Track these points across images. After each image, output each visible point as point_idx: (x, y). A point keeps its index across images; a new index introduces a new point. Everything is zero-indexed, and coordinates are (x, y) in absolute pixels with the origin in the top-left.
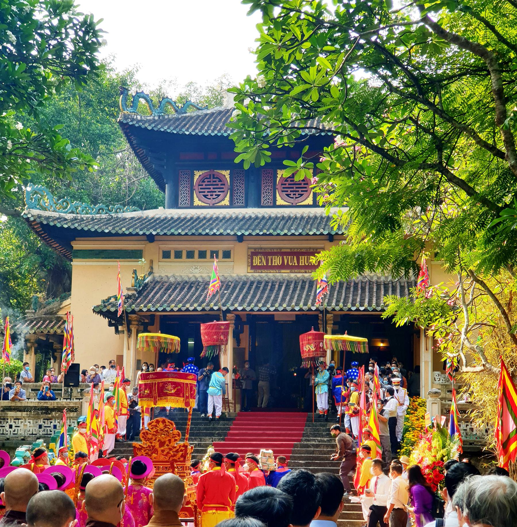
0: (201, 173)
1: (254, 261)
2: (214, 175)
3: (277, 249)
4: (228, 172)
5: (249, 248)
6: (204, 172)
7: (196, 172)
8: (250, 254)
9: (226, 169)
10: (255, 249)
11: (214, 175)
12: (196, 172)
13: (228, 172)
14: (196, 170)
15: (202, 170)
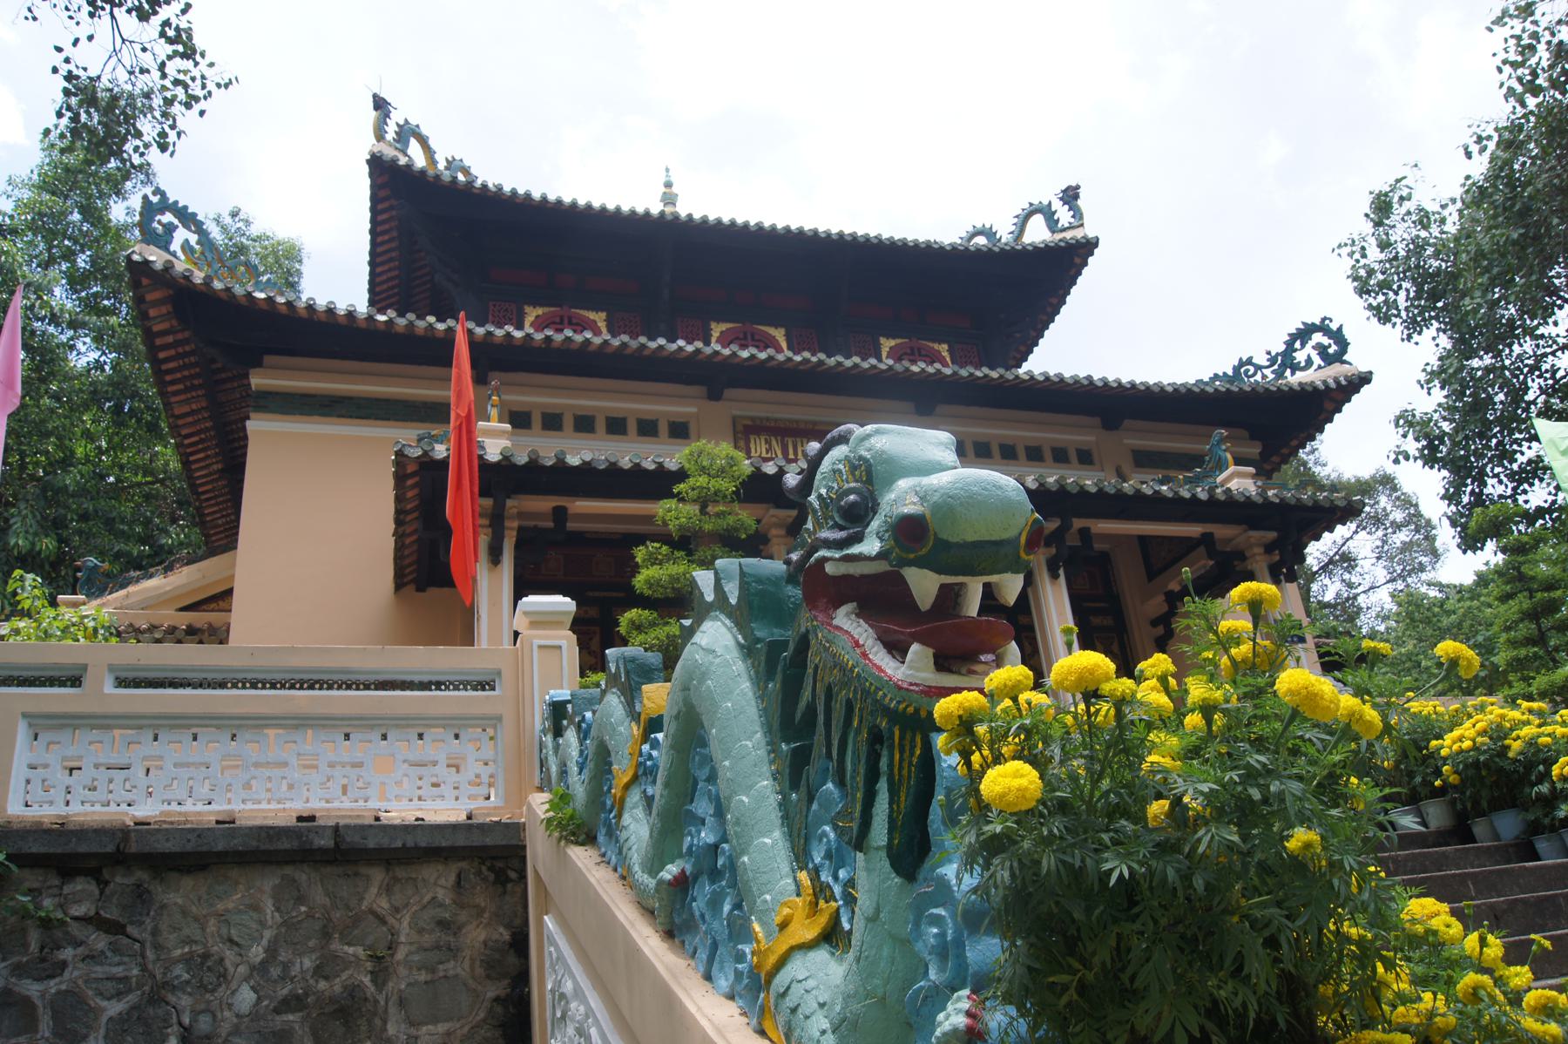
0: (540, 311)
1: (752, 446)
2: (570, 319)
3: (806, 422)
4: (603, 315)
5: (735, 420)
6: (547, 310)
7: (528, 309)
8: (739, 428)
9: (597, 310)
10: (752, 419)
11: (570, 319)
12: (528, 309)
13: (603, 315)
14: (529, 304)
15: (541, 305)
